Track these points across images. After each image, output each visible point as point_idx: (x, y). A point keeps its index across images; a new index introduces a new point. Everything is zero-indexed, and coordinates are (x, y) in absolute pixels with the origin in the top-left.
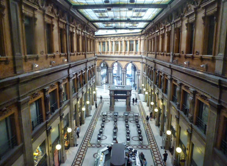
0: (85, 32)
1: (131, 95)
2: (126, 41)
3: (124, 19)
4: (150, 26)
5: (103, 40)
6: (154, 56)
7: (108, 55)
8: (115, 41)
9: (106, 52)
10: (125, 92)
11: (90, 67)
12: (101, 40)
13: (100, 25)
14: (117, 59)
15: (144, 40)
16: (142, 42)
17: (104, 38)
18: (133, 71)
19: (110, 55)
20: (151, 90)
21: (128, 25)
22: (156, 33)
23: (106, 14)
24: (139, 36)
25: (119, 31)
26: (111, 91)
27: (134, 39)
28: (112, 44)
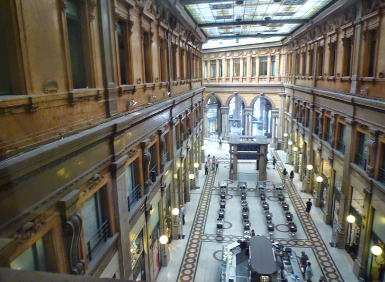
0: (190, 43)
1: (266, 152)
2: (253, 59)
3: (259, 18)
4: (304, 29)
5: (213, 57)
6: (310, 83)
7: (222, 83)
8: (234, 58)
9: (217, 77)
10: (256, 147)
11: (196, 105)
12: (208, 57)
13: (216, 31)
14: (237, 90)
15: (288, 55)
16: (284, 58)
17: (214, 55)
18: (264, 111)
19: (224, 84)
20: (305, 144)
21: (260, 29)
22: (317, 41)
23: (230, 12)
24: (277, 48)
25: (243, 41)
26: (231, 145)
27: (269, 54)
28: (228, 65)
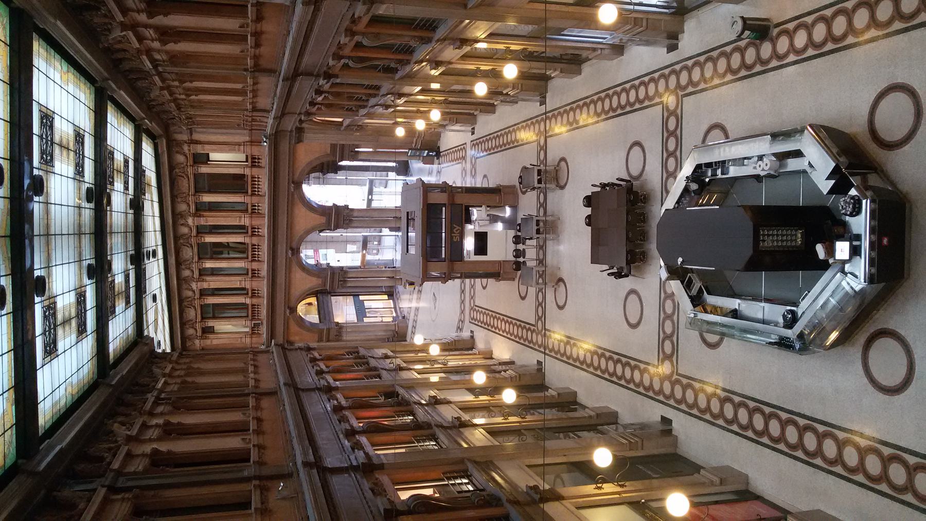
0: (151, 398)
1: (445, 188)
2: (201, 209)
3: (88, 214)
4: (124, 97)
6: (265, 82)
7: (263, 287)
8: (196, 259)
9: (248, 301)
10: (431, 211)
11: (320, 373)
13: (120, 327)
15: (194, 123)
17: (187, 310)
19: (265, 282)
20: (422, 92)
21: (119, 200)
22: (155, 67)
23: (65, 302)
25: (153, 239)
26: (426, 277)
27: (190, 170)
28: (214, 272)
